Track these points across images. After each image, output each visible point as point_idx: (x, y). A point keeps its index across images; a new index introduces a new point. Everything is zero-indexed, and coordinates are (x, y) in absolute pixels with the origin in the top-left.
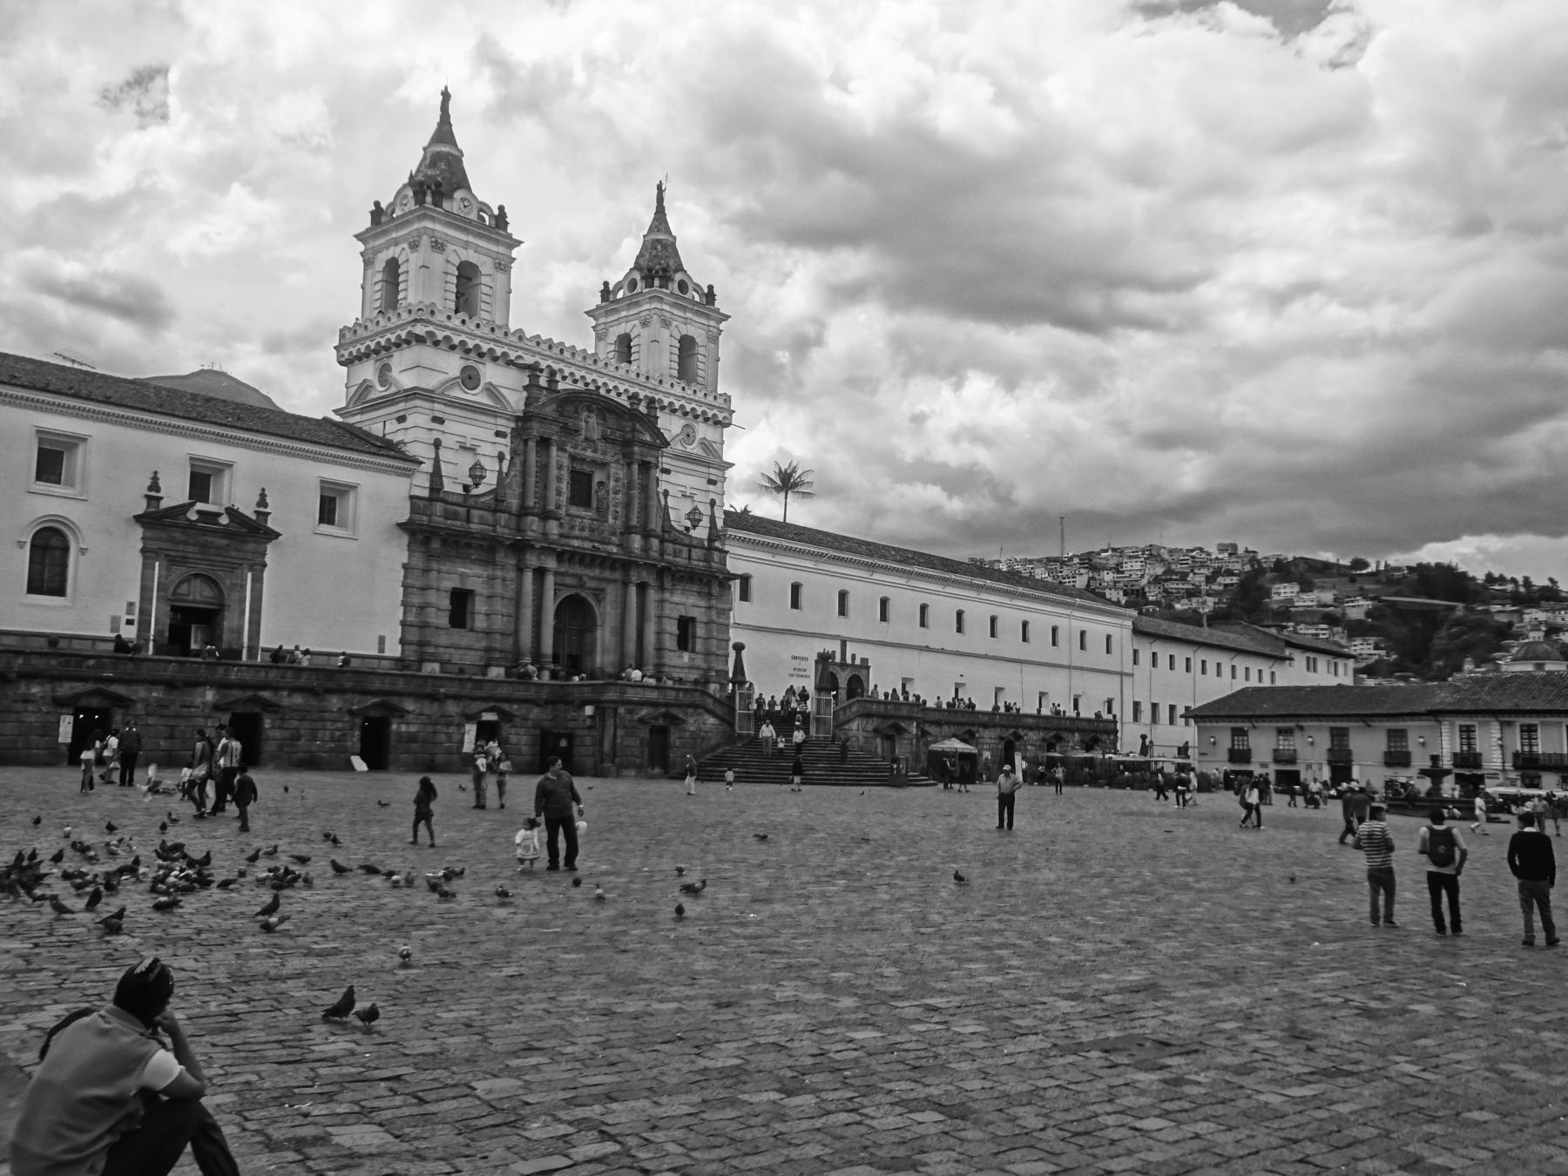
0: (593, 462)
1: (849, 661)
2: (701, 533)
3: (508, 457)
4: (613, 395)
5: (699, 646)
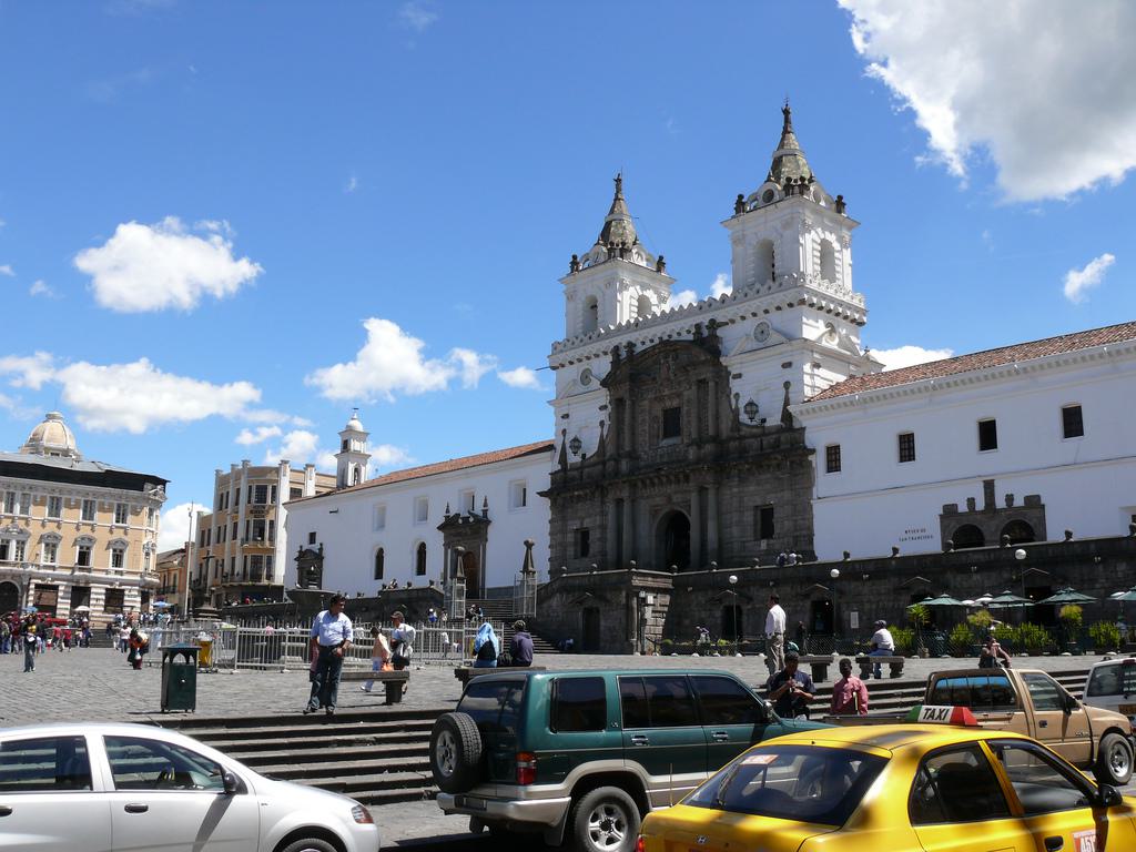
0: (670, 397)
1: (1000, 503)
2: (774, 420)
3: (607, 423)
4: (675, 337)
5: (777, 530)
